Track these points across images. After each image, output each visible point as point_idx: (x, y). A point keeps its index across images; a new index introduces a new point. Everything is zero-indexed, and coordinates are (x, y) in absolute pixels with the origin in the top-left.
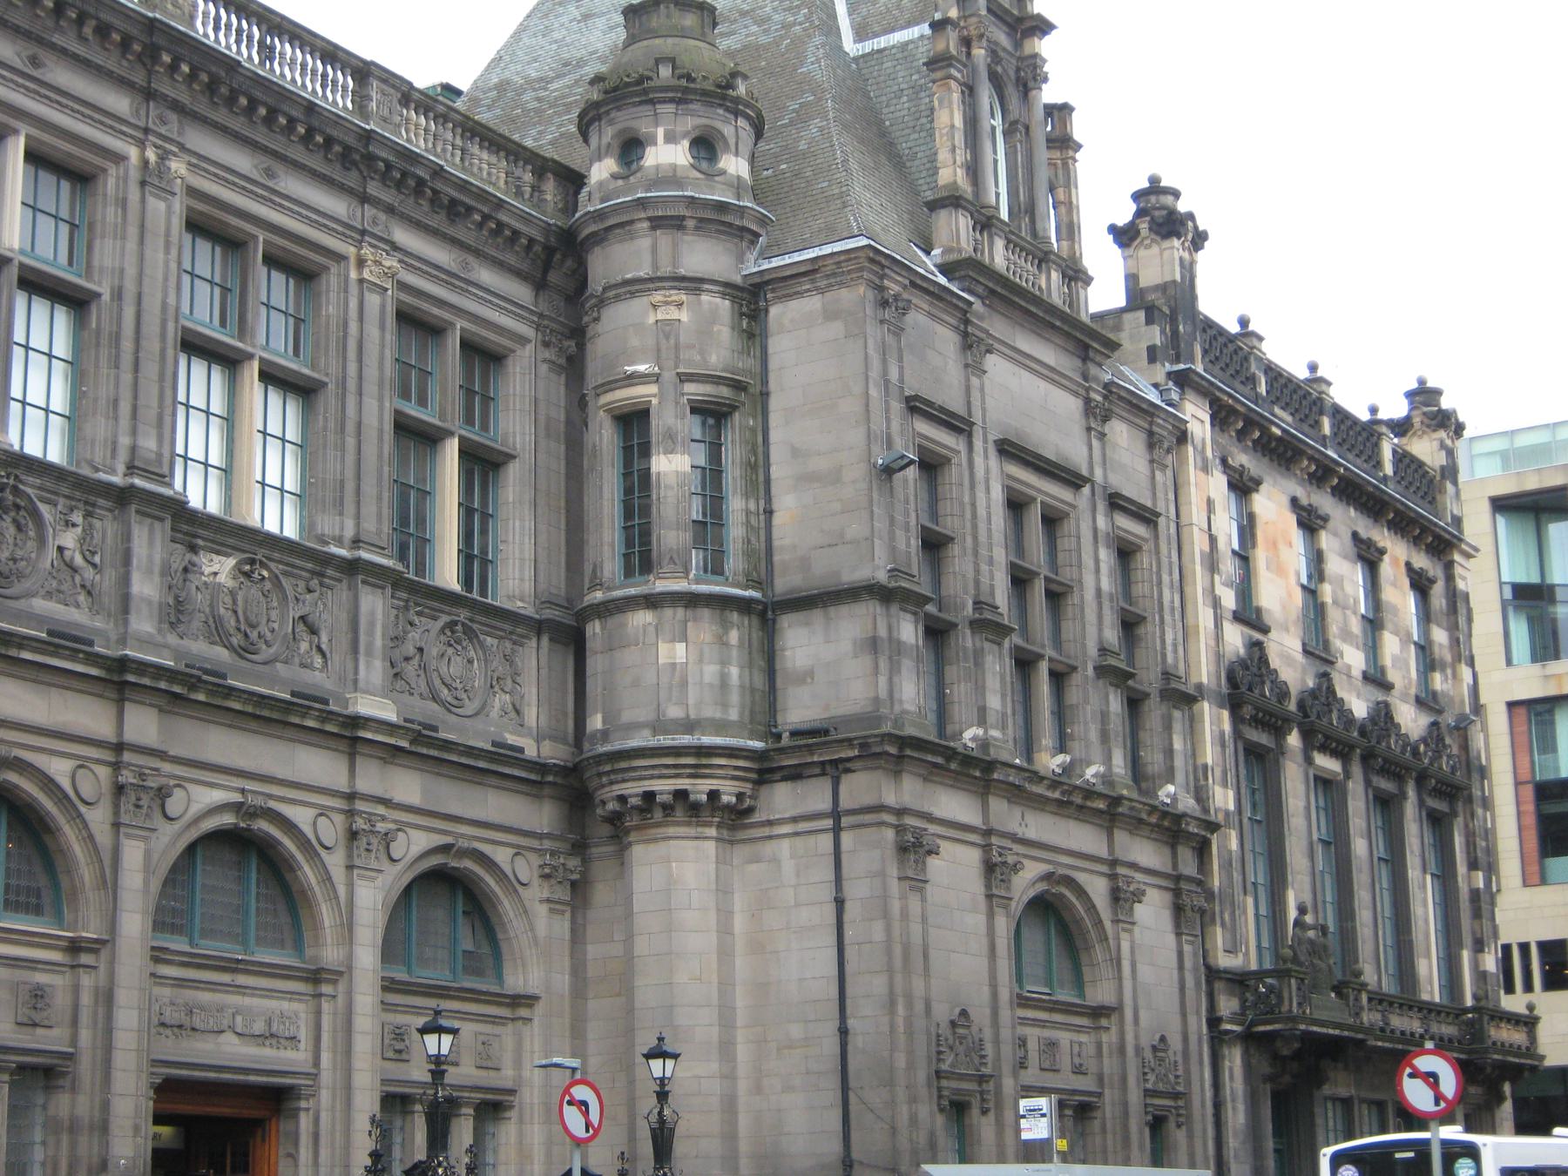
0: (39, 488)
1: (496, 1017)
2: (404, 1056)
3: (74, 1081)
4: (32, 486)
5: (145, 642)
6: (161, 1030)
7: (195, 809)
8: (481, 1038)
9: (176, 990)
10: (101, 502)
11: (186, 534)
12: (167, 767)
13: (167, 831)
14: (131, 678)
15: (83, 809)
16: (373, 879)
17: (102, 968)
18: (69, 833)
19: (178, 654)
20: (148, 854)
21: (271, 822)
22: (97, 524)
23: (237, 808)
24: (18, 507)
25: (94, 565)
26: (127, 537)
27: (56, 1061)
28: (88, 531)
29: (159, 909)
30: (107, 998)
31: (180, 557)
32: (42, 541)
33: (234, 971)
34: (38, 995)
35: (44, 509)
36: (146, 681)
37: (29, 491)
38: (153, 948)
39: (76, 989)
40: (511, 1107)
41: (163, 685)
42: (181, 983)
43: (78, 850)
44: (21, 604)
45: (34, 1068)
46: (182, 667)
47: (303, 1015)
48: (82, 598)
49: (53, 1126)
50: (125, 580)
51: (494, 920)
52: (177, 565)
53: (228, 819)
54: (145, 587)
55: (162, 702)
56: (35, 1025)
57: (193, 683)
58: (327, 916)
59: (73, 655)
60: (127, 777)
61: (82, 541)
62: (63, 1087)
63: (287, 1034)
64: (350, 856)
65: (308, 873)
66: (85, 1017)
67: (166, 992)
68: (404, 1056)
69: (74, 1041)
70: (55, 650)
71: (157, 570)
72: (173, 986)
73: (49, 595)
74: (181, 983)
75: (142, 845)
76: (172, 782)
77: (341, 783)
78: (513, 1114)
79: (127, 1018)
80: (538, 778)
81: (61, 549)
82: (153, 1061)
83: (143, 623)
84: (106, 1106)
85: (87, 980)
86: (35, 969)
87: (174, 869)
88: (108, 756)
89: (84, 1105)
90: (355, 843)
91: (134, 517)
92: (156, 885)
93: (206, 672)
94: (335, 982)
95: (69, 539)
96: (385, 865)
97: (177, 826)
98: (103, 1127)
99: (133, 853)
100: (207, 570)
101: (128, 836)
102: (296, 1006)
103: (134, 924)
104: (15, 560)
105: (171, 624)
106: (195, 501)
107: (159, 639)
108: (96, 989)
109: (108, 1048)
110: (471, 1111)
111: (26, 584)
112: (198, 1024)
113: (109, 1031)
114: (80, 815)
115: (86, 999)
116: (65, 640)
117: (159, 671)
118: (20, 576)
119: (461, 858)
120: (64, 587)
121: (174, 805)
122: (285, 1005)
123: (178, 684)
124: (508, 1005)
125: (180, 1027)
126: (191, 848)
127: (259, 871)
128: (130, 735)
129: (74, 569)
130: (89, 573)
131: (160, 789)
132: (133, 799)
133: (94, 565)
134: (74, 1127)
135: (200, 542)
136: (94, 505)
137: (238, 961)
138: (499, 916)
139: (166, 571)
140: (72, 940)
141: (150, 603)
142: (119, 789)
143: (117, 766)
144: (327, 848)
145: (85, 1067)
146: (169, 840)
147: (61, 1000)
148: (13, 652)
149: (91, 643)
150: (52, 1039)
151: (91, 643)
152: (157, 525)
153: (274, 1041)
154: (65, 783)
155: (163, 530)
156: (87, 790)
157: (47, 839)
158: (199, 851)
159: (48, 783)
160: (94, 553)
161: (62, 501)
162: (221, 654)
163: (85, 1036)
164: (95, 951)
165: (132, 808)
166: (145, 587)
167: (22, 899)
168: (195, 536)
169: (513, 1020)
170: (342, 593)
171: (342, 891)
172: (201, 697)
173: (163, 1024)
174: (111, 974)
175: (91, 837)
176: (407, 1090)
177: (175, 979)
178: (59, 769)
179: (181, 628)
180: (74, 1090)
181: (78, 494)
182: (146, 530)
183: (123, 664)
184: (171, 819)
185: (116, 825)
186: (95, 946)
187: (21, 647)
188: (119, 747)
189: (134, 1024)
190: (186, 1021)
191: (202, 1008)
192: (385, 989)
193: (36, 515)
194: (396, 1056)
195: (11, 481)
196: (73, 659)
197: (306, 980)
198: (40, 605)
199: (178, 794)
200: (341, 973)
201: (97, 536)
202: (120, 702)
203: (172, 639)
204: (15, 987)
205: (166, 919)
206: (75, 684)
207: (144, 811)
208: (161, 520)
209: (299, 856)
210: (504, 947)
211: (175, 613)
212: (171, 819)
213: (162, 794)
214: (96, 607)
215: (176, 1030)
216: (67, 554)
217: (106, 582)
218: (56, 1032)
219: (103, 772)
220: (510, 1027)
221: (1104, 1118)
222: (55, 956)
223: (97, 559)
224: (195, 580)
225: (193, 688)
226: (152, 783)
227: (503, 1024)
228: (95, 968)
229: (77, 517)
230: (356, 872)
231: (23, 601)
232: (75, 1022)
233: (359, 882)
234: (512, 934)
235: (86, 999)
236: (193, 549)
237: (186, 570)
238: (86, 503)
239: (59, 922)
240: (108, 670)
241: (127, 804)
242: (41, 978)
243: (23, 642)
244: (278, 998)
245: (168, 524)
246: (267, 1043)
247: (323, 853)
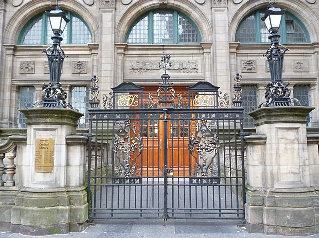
1: (303, 53)
2: (253, 71)
6: (132, 70)
8: (297, 61)
9: (138, 58)
16: (224, 11)
27: (86, 83)
33: (164, 49)
34: (80, 64)
40: (314, 85)
47: (199, 61)
51: (302, 21)
58: (205, 27)
62: (314, 89)
63: (191, 68)
65: (195, 15)
68: (253, 71)
75: (111, 14)
78: (316, 87)
94: (210, 48)
99: (107, 17)
102: (196, 58)
112: (148, 67)
122: (191, 58)
124: (310, 49)
125: (141, 69)
137: (164, 46)
138: (302, 17)
147: (90, 65)
153: (185, 71)
164: (97, 49)
165: (104, 3)
169: (313, 53)
171: (209, 17)
173: (132, 69)
177: (137, 54)
184: (93, 4)
189: (110, 68)
190: (144, 67)
191: (150, 62)
192: (230, 48)
194: (249, 71)
197: (199, 49)
200: (211, 44)
209: (190, 10)
210: (308, 29)
212: (93, 4)
220: (313, 56)
221: (215, 56)
222: (87, 52)
227: (310, 56)
228: (97, 54)
233: (216, 13)
234: (309, 23)
242: (81, 60)
244: (186, 56)
246: (182, 71)
247: (199, 6)
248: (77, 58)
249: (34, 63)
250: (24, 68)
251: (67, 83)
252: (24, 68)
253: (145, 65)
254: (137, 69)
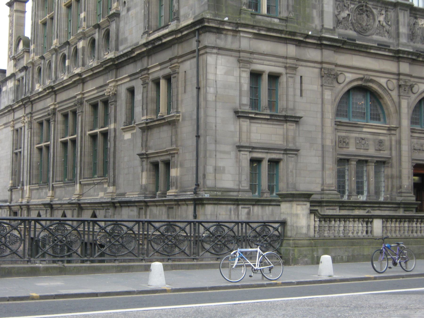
0: (373, 5)
3: (391, 164)
4: (371, 5)
5: (404, 45)
6: (415, 151)
7: (348, 80)
10: (389, 7)
11: (414, 14)
12: (412, 79)
13: (413, 97)
14: (401, 55)
15: (390, 92)
17: (397, 135)
18: (387, 98)
19: (413, 48)
20: (408, 103)
21: (373, 83)
22: (389, 13)
23: (361, 79)
24: (367, 11)
25: (389, 25)
26: (398, 16)
27: (387, 160)
28: (386, 16)
29: (338, 110)
30: (399, 142)
31: (413, 20)
32: (374, 19)
34: (381, 142)
35: (375, 11)
36: (405, 56)
37: (370, 6)
38: (335, 121)
39: (391, 141)
41: (410, 56)
42: (419, 138)
43: (389, 103)
44: (369, 37)
45: (344, 159)
46: (341, 39)
48: (386, 34)
49: (387, 177)
50: (398, 28)
52: (412, 22)
53: (360, 83)
54: (403, 30)
55: (410, 61)
56: (380, 150)
57: (344, 43)
59: (385, 50)
60: (402, 83)
61: (385, 18)
64: (399, 92)
66: (393, 148)
67: (415, 141)
69: (391, 154)
70: (380, 49)
71: (406, 24)
72: (417, 139)
73: (377, 34)
74: (419, 138)
76: (414, 83)
77: (319, 59)
79: (405, 148)
80: (319, 42)
81: (379, 21)
82: (338, 154)
83: (403, 40)
84: (400, 171)
85: (393, 138)
86: (379, 135)
87: (342, 98)
88: (396, 77)
89: (395, 171)
90: (401, 88)
91: (399, 11)
92: (411, 111)
93: (348, 39)
95: (382, 18)
96: (336, 84)
97: (342, 85)
98: (400, 177)
99: (404, 103)
100: (420, 24)
101: (326, 89)
103: (405, 122)
104: (367, 26)
105: (412, 40)
106: (415, 4)
107: (408, 44)
108: (396, 141)
109: (400, 156)
110: (355, 163)
111: (371, 32)
113: (400, 151)
114: (389, 94)
115: (394, 143)
116: (382, 46)
117: (409, 53)
118: (369, 29)
119: (367, 82)
120: (381, 32)
121: (341, 79)
123: (263, 31)
125: (419, 150)
126: (348, 92)
127: (370, 98)
128: (402, 71)
129: (383, 27)
130: (388, 27)
131: (411, 85)
132: (403, 88)
133: (389, 25)
134: (392, 177)
135: (418, 16)
136: (388, 8)
139: (409, 25)
140: (389, 127)
141: (405, 34)
142: (400, 86)
143: (398, 80)
144: (391, 90)
145: (394, 161)
146: (414, 99)
147: (387, 143)
148: (368, 51)
149: (389, 46)
150: (385, 154)
151: (389, 46)
152: (406, 12)
154: (385, 85)
155: (407, 13)
156: (391, 87)
157: (381, 101)
158: (351, 93)
159: (380, 85)
160: (388, 22)
161: (379, 8)
162: (351, 33)
163: (394, 153)
164: (395, 130)
165: (403, 91)
166: (403, 30)
167: (375, 117)
168: (416, 14)
170: (392, 14)
172: (421, 59)
173: (415, 149)
174: (400, 136)
175: (393, 100)
176: (349, 157)
178: (383, 81)
179: (414, 41)
180: (392, 167)
181: (383, 6)
182: (402, 14)
183: (398, 51)
185: (399, 96)
186: (395, 129)
187: (370, 49)
188: (399, 74)
190: (421, 148)
193: (372, 12)
195: (365, 4)
196: (385, 51)
198: (375, 37)
199: (416, 87)
201: (389, 17)
202: (398, 62)
203: (412, 44)
204: (374, 140)
205: (414, 121)
206: (386, 58)
207: (407, 91)
208: (407, 11)
211: (412, 36)
212: (414, 93)
213: (411, 87)
214: (390, 37)
215: (418, 151)
216: (381, 23)
217: (393, 29)
218: (386, 152)
219: (395, 82)
223: (389, 23)
224: (417, 27)
225: (418, 57)
226: (332, 73)
229: (383, 12)
230: (324, 87)
231: (370, 36)
232: (391, 149)
235: (394, 143)
236: (416, 18)
237: (414, 24)
238: (385, 8)
239: (385, 122)
240: (318, 40)
241: (402, 90)
242: (381, 138)
243: (371, 47)
245: (409, 11)
248: (378, 137)
249: (347, 137)
250: (342, 142)
251: (373, 159)
252: (342, 142)
253: (422, 146)
254: (417, 150)
